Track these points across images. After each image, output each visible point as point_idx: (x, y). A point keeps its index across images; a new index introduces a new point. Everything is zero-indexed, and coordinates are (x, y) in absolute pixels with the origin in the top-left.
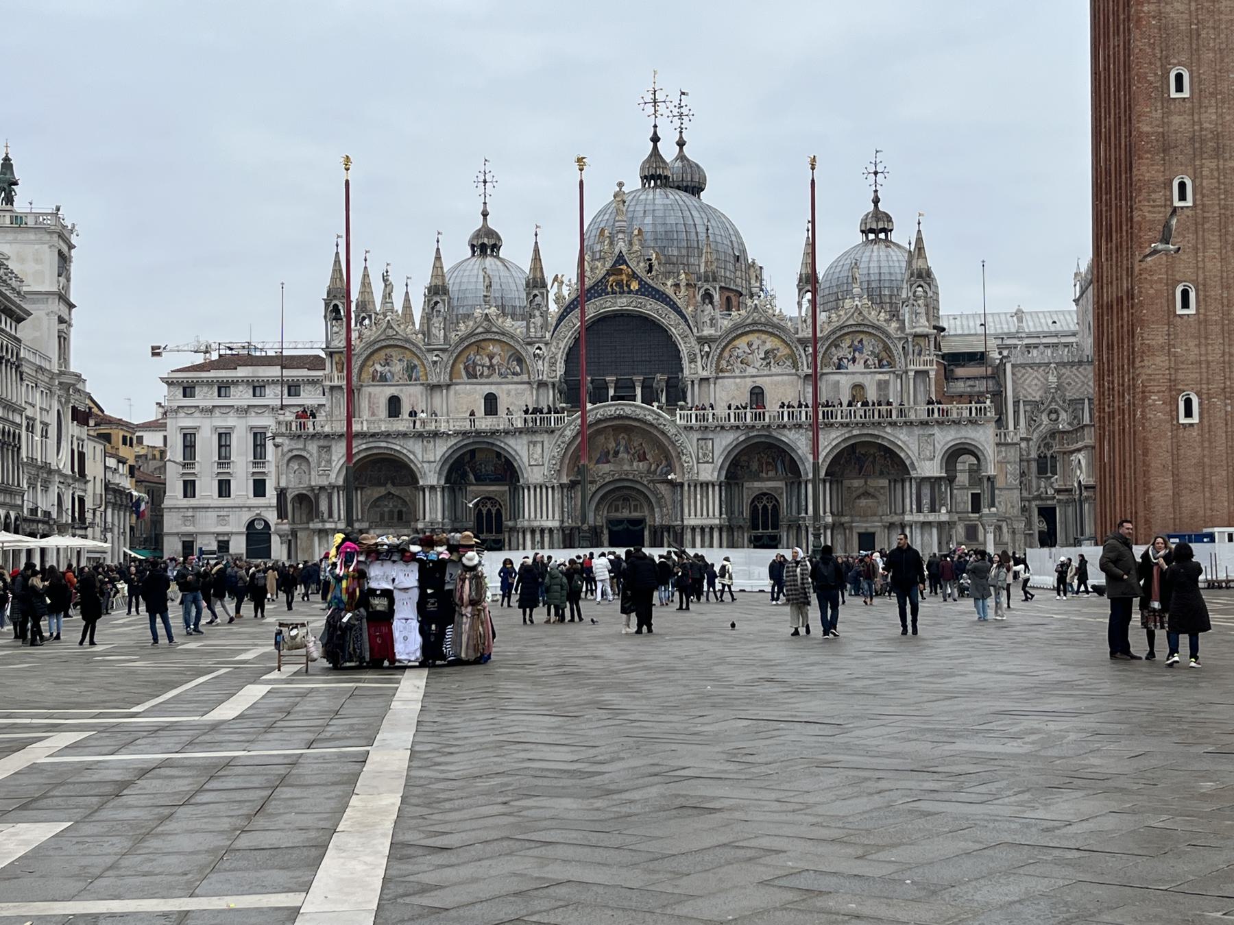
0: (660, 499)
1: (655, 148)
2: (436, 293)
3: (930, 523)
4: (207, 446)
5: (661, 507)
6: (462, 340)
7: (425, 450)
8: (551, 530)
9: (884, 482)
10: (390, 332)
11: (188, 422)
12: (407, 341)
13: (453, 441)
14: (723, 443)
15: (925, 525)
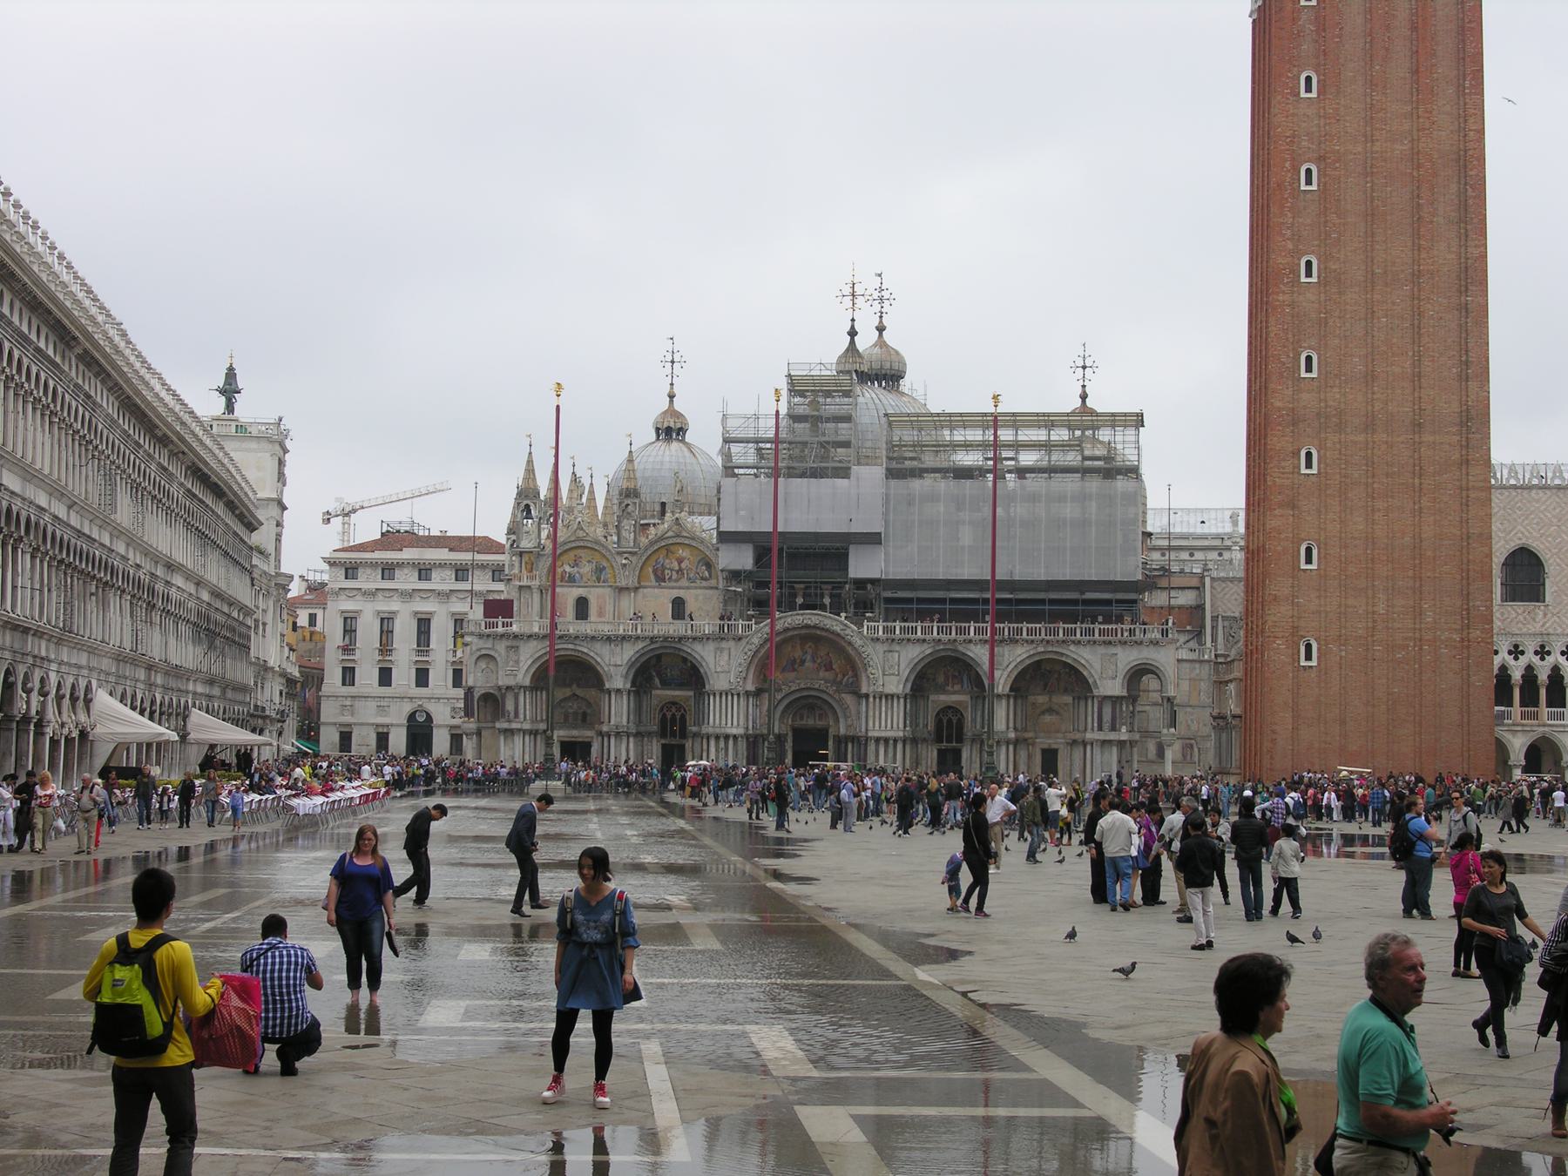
0: (846, 709)
1: (852, 342)
2: (627, 496)
3: (1110, 742)
4: (368, 632)
5: (846, 717)
6: (652, 543)
7: (613, 653)
8: (735, 737)
9: (1068, 699)
10: (581, 534)
11: (349, 605)
12: (597, 542)
13: (640, 645)
14: (909, 657)
15: (1104, 742)
